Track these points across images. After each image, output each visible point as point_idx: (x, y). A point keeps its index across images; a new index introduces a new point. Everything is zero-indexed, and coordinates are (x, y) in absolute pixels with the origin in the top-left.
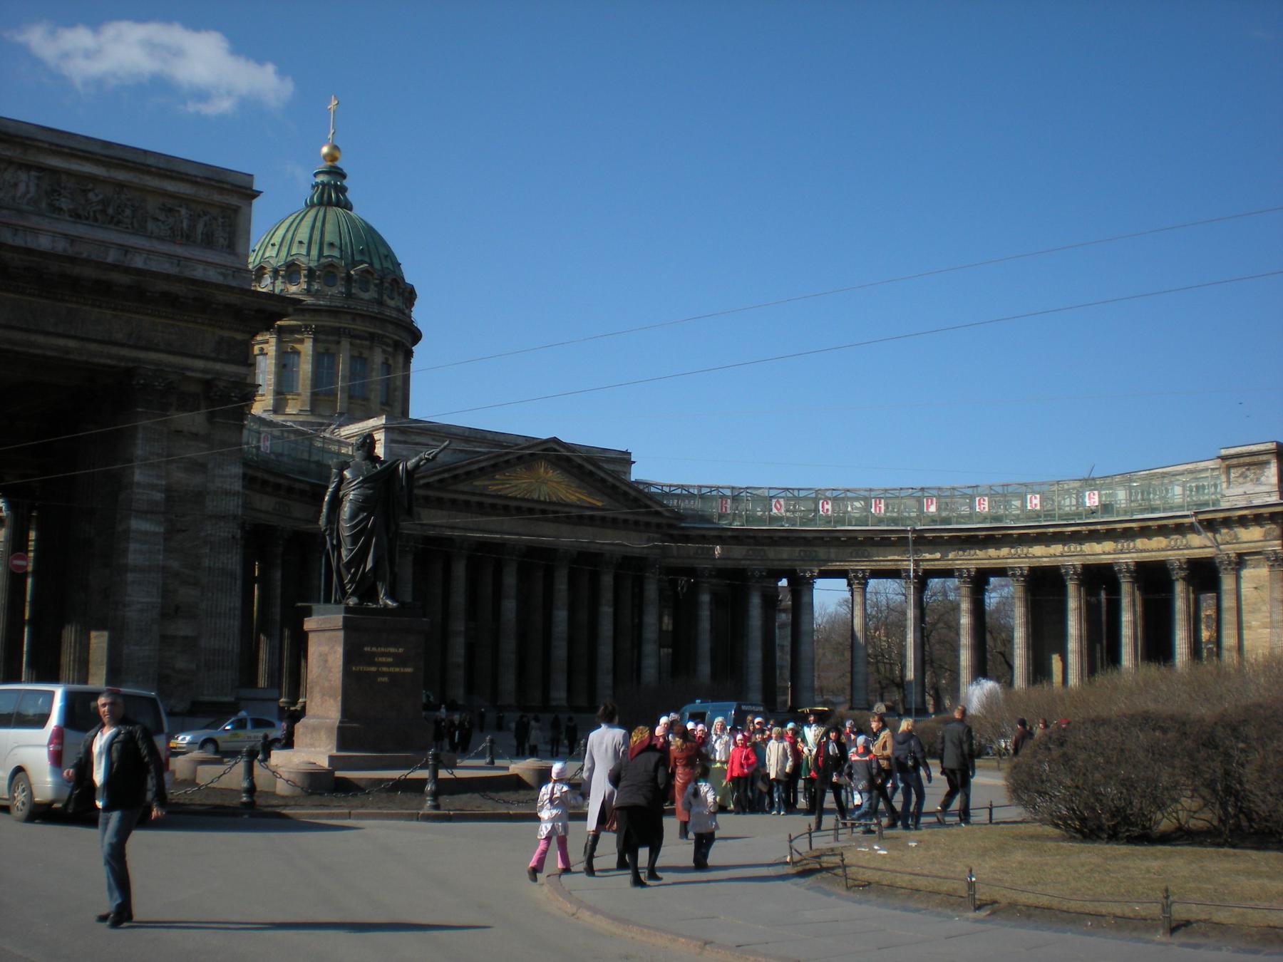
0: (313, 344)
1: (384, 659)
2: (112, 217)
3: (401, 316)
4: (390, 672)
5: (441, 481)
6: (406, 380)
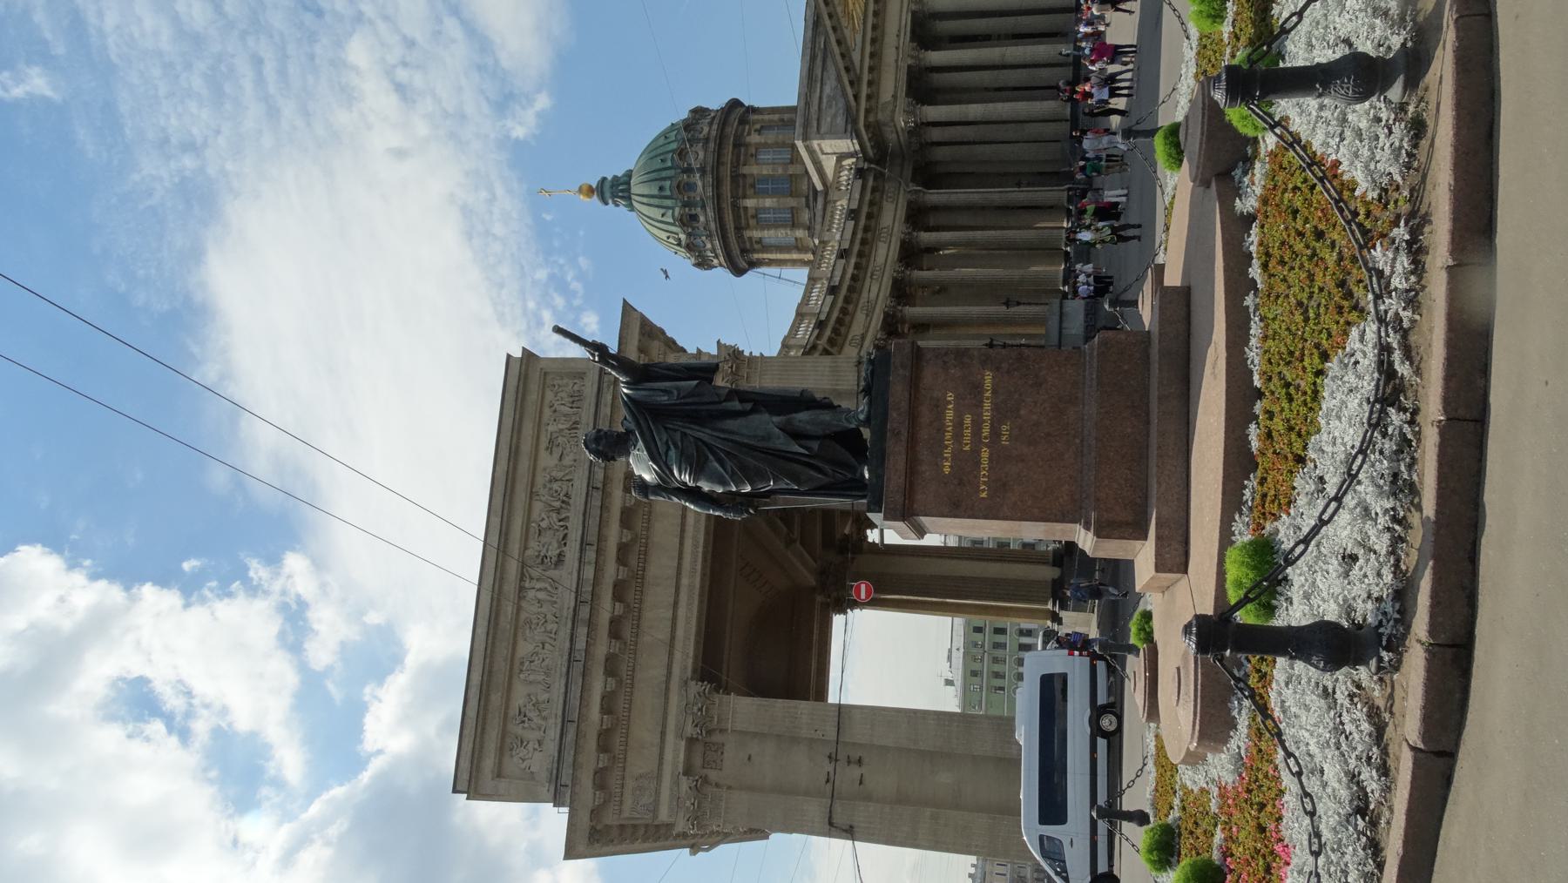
0: (749, 198)
1: (967, 432)
2: (563, 502)
3: (716, 121)
4: (993, 417)
5: (852, 83)
6: (773, 110)
